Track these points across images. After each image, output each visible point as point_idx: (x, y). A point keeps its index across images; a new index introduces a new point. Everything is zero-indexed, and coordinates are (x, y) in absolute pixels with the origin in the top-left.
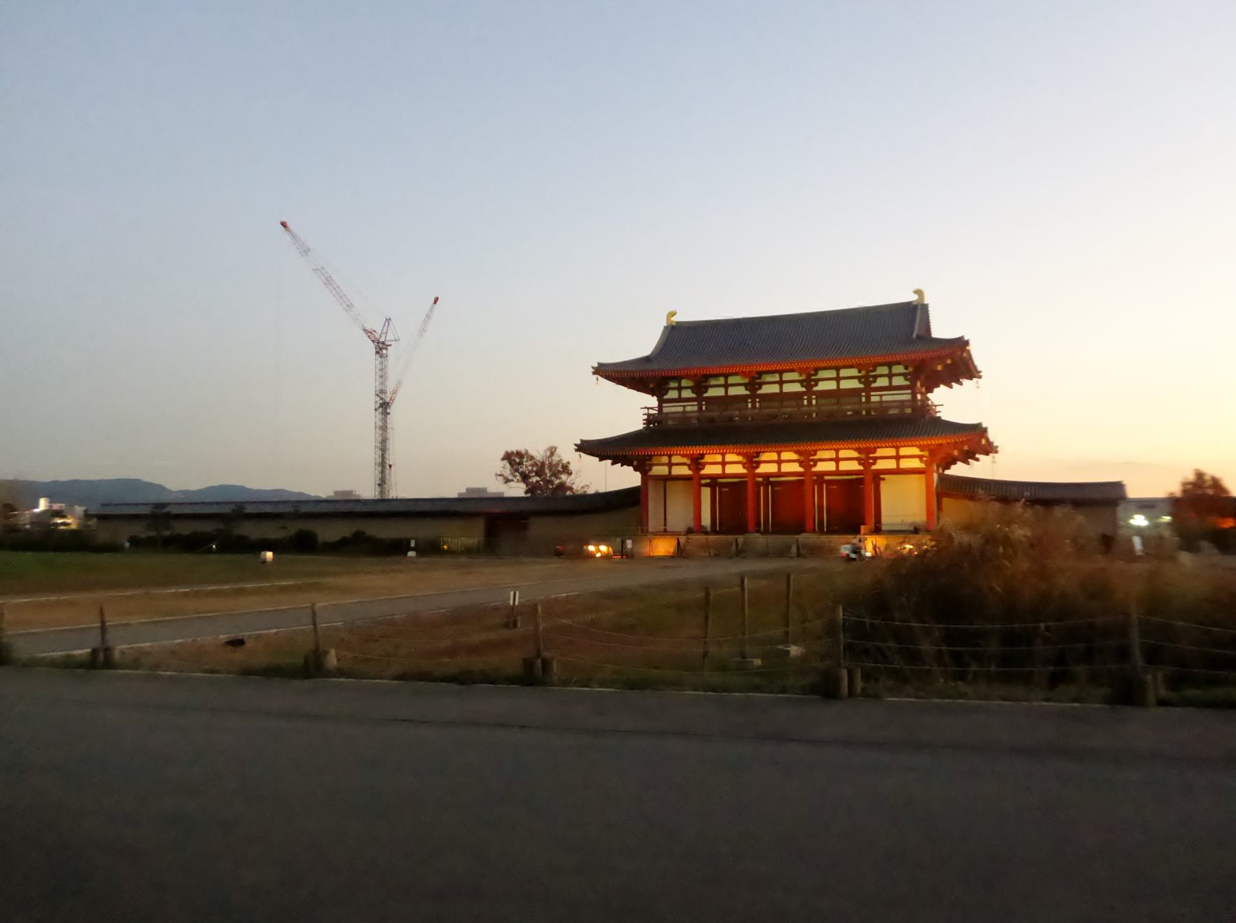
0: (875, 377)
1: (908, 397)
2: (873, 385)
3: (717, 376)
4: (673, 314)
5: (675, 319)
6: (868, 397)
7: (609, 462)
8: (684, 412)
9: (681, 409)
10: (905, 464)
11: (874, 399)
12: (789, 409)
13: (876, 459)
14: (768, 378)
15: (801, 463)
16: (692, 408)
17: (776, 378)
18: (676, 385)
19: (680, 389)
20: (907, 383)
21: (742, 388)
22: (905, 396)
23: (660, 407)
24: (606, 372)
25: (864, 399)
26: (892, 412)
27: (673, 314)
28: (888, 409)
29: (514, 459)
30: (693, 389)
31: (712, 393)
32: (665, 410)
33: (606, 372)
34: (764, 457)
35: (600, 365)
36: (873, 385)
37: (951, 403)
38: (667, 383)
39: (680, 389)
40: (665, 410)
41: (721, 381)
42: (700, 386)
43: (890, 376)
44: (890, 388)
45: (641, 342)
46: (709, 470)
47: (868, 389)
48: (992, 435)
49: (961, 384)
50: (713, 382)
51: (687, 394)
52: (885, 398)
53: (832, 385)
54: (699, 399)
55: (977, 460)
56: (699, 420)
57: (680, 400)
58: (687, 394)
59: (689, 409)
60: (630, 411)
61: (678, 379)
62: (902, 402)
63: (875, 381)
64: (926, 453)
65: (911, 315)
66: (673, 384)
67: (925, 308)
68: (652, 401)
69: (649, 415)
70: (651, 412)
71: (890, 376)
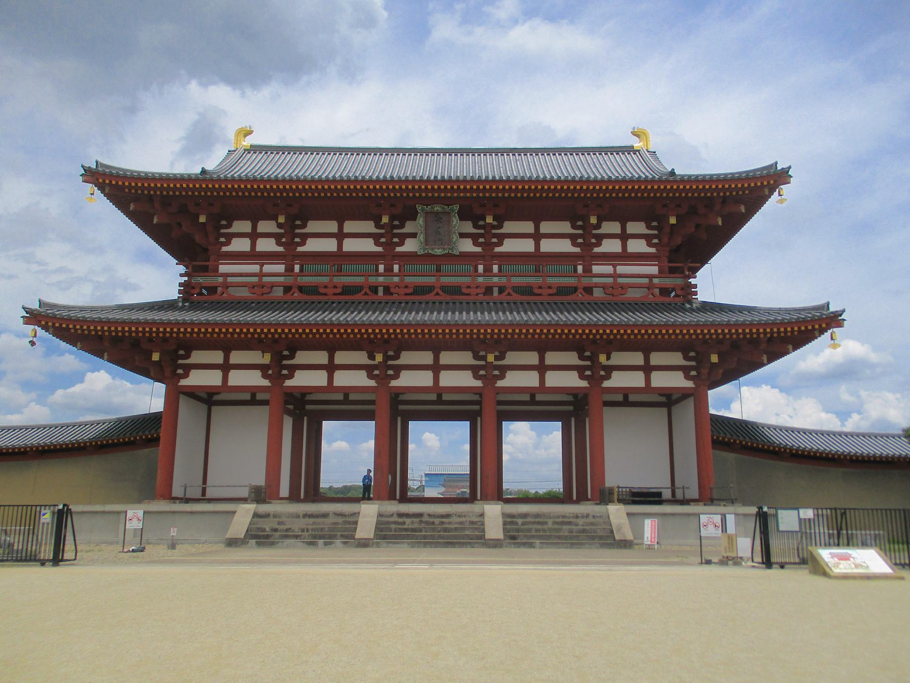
0: (600, 238)
6: (587, 270)
8: (261, 275)
9: (255, 268)
19: (254, 236)
26: (633, 294)
28: (624, 287)
30: (277, 237)
31: (313, 246)
43: (624, 237)
44: (625, 257)
47: (588, 257)
52: (621, 269)
54: (289, 256)
56: (287, 289)
57: (253, 256)
58: (266, 245)
59: (268, 268)
62: (651, 277)
71: (624, 237)
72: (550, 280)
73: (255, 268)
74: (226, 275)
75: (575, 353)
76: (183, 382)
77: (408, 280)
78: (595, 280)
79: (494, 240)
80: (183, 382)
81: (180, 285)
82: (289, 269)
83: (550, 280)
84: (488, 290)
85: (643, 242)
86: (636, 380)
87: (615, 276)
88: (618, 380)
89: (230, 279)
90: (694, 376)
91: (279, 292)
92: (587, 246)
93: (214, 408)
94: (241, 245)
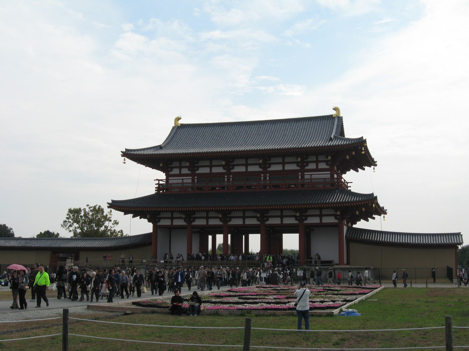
1: (328, 176)
2: (306, 168)
4: (178, 119)
5: (180, 122)
6: (303, 176)
7: (130, 215)
9: (180, 181)
10: (326, 220)
11: (306, 177)
16: (188, 180)
20: (328, 167)
22: (327, 175)
23: (167, 180)
24: (129, 154)
25: (300, 177)
27: (178, 119)
29: (74, 213)
32: (170, 182)
33: (129, 154)
35: (127, 150)
36: (306, 168)
37: (358, 181)
40: (170, 182)
44: (317, 170)
45: (154, 136)
47: (303, 171)
48: (381, 203)
49: (364, 169)
51: (185, 171)
52: (313, 177)
54: (193, 175)
55: (374, 218)
56: (192, 189)
57: (180, 175)
58: (185, 171)
59: (185, 181)
60: (145, 182)
62: (325, 179)
63: (307, 165)
64: (338, 213)
65: (334, 122)
67: (340, 119)
68: (162, 175)
69: (158, 184)
70: (161, 182)
74: (171, 184)
76: (159, 224)
78: (306, 181)
80: (159, 224)
81: (156, 188)
82: (193, 180)
84: (265, 187)
85: (324, 164)
89: (173, 185)
91: (190, 190)
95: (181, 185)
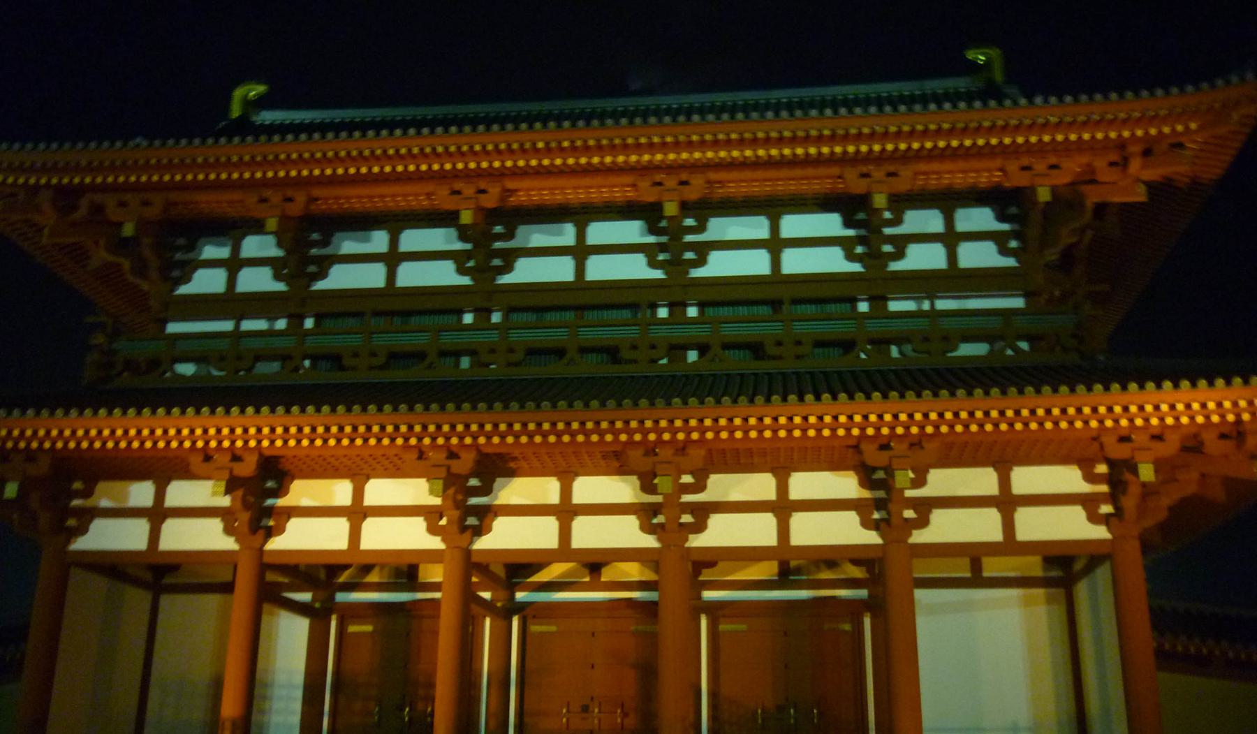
3: (363, 223)
8: (237, 335)
9: (227, 326)
12: (613, 329)
13: (926, 507)
14: (538, 237)
15: (645, 513)
17: (566, 235)
18: (223, 252)
21: (449, 266)
34: (514, 491)
38: (192, 246)
39: (234, 265)
41: (379, 241)
42: (303, 257)
46: (304, 536)
50: (349, 246)
53: (756, 264)
58: (256, 280)
61: (232, 228)
66: (211, 251)
72: (799, 328)
73: (227, 326)
75: (851, 473)
77: (515, 336)
79: (689, 255)
83: (799, 328)
86: (983, 526)
87: (934, 314)
88: (945, 527)
90: (1108, 516)
92: (874, 258)
93: (166, 601)
94: (208, 282)
95: (223, 344)
